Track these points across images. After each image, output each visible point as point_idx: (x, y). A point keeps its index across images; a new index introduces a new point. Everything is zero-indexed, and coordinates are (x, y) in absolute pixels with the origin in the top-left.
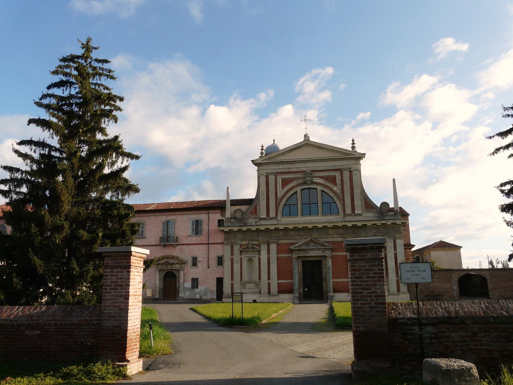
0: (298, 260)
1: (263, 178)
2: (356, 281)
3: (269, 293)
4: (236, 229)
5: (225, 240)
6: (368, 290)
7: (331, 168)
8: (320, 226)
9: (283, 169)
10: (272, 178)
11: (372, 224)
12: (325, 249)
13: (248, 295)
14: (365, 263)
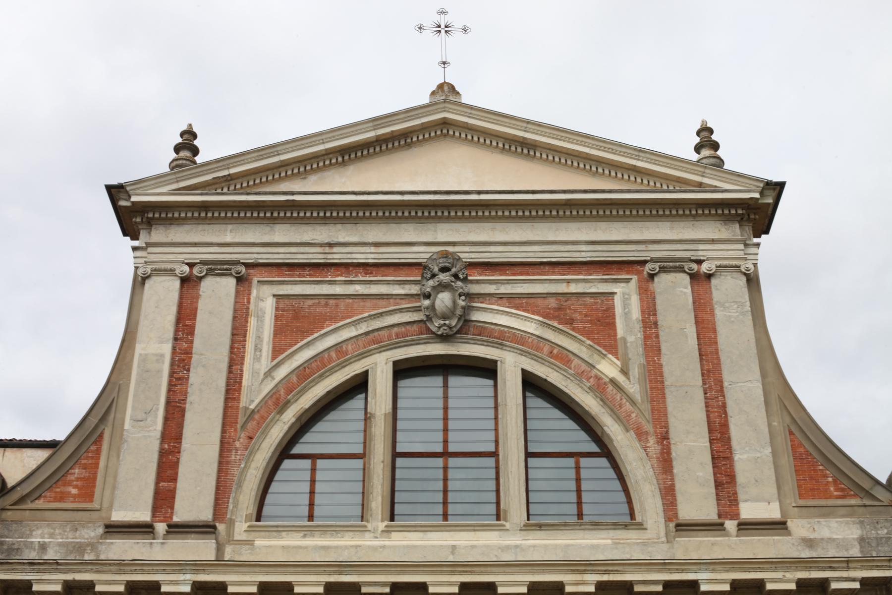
9: (293, 249)
11: (864, 581)
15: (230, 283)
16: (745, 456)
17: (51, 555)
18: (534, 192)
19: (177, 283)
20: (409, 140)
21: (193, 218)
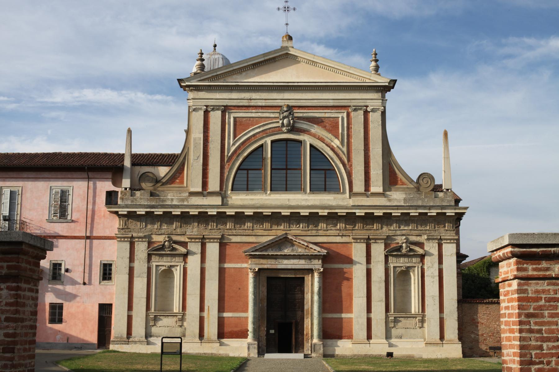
0: (259, 276)
1: (199, 117)
2: (529, 323)
3: (201, 336)
4: (141, 211)
5: (119, 232)
6: (554, 342)
7: (331, 103)
8: (305, 212)
9: (239, 101)
10: (215, 117)
11: (402, 213)
14: (548, 285)
15: (219, 113)
16: (374, 173)
17: (175, 203)
20: (275, 60)
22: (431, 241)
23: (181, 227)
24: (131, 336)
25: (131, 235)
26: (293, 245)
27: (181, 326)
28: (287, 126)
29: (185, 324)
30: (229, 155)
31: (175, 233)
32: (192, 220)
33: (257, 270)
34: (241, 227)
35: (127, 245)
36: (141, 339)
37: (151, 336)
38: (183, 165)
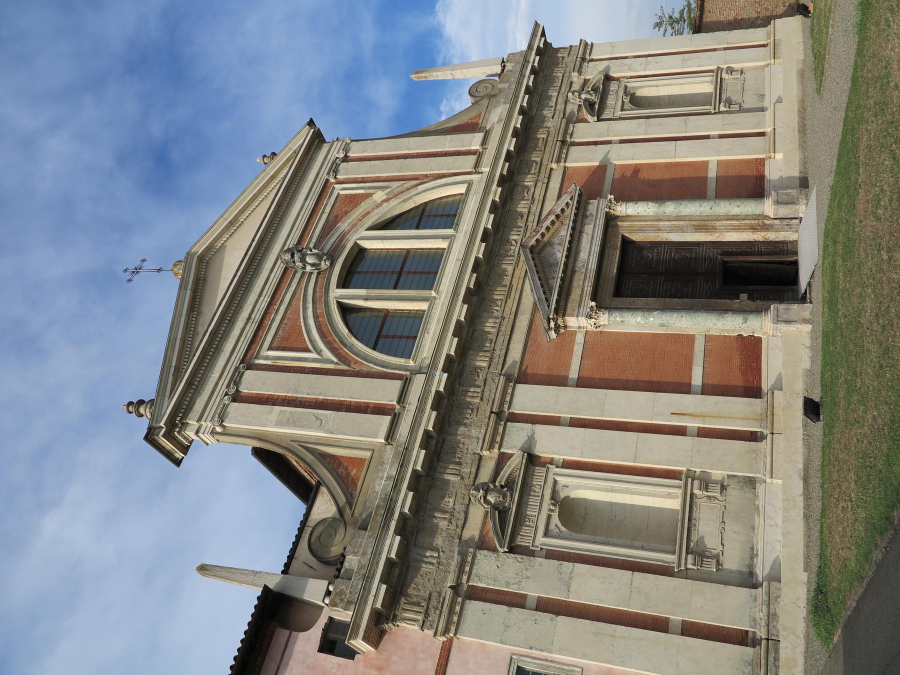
12: (581, 211)
13: (759, 546)
18: (265, 216)
19: (234, 404)
21: (193, 394)
22: (583, 70)
23: (460, 464)
24: (750, 635)
25: (449, 591)
26: (549, 243)
27: (723, 488)
28: (321, 260)
29: (717, 474)
30: (335, 360)
31: (472, 480)
32: (449, 438)
33: (593, 304)
34: (491, 340)
35: (474, 608)
36: (759, 601)
37: (751, 574)
38: (324, 457)
